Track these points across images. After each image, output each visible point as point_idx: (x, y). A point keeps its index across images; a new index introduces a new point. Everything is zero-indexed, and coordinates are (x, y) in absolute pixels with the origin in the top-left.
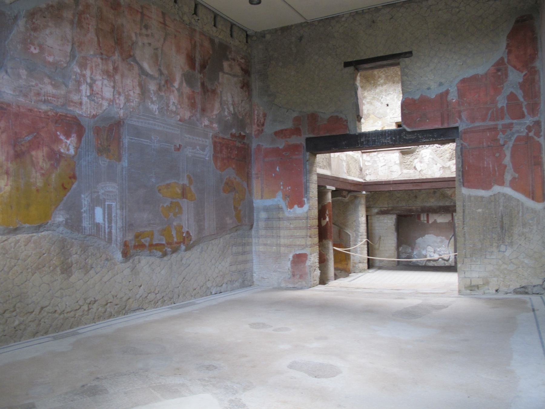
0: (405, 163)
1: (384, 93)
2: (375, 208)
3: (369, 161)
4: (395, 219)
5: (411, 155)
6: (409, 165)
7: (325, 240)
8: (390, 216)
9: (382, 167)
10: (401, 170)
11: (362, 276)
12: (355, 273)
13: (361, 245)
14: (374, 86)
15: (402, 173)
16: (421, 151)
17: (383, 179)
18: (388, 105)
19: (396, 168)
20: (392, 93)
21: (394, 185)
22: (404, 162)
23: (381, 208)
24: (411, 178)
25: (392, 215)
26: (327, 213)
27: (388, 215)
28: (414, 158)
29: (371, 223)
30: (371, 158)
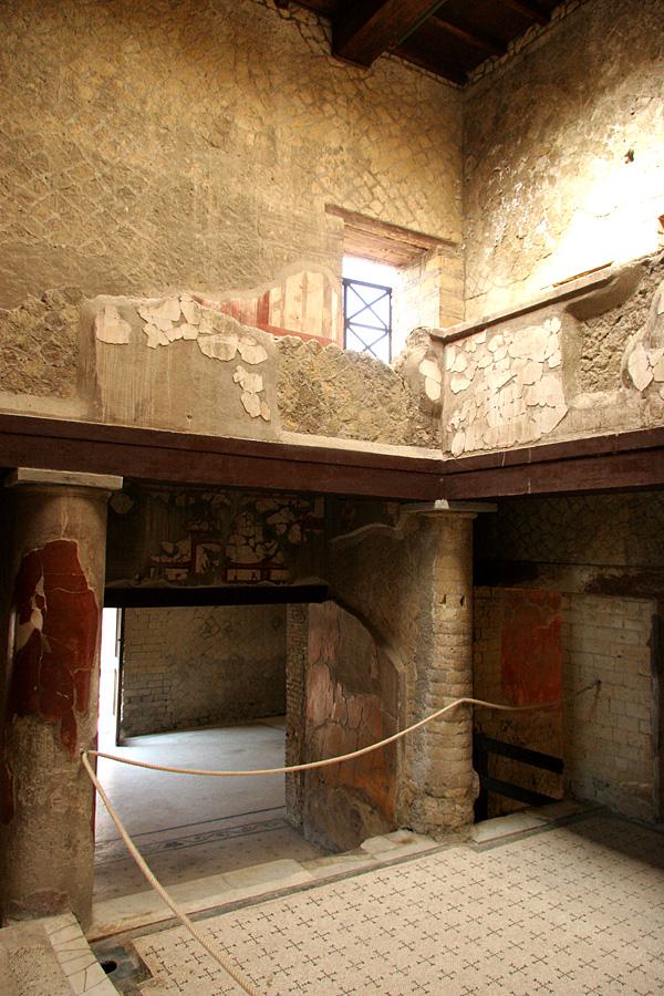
0: (591, 359)
1: (619, 115)
2: (581, 567)
3: (461, 374)
4: (654, 616)
5: (615, 314)
6: (604, 367)
7: (21, 716)
8: (634, 605)
9: (500, 389)
10: (570, 393)
11: (428, 853)
12: (411, 830)
13: (435, 719)
14: (584, 102)
15: (571, 409)
16: (658, 284)
17: (501, 444)
18: (630, 156)
19: (549, 389)
20: (646, 100)
21: (539, 470)
22: (586, 358)
23: (601, 567)
24: (607, 429)
25: (642, 600)
26: (40, 590)
27: (627, 599)
28: (626, 326)
29: (571, 625)
30: (470, 360)
